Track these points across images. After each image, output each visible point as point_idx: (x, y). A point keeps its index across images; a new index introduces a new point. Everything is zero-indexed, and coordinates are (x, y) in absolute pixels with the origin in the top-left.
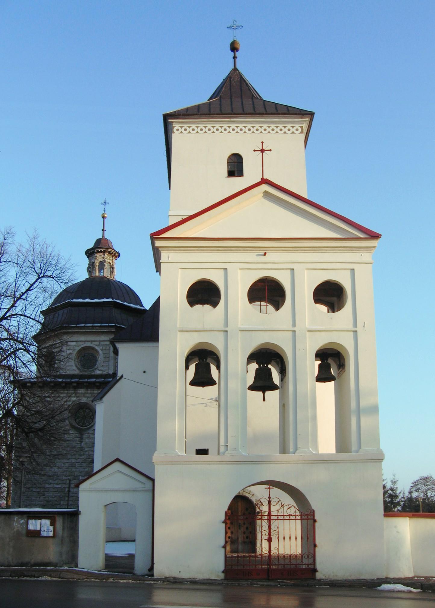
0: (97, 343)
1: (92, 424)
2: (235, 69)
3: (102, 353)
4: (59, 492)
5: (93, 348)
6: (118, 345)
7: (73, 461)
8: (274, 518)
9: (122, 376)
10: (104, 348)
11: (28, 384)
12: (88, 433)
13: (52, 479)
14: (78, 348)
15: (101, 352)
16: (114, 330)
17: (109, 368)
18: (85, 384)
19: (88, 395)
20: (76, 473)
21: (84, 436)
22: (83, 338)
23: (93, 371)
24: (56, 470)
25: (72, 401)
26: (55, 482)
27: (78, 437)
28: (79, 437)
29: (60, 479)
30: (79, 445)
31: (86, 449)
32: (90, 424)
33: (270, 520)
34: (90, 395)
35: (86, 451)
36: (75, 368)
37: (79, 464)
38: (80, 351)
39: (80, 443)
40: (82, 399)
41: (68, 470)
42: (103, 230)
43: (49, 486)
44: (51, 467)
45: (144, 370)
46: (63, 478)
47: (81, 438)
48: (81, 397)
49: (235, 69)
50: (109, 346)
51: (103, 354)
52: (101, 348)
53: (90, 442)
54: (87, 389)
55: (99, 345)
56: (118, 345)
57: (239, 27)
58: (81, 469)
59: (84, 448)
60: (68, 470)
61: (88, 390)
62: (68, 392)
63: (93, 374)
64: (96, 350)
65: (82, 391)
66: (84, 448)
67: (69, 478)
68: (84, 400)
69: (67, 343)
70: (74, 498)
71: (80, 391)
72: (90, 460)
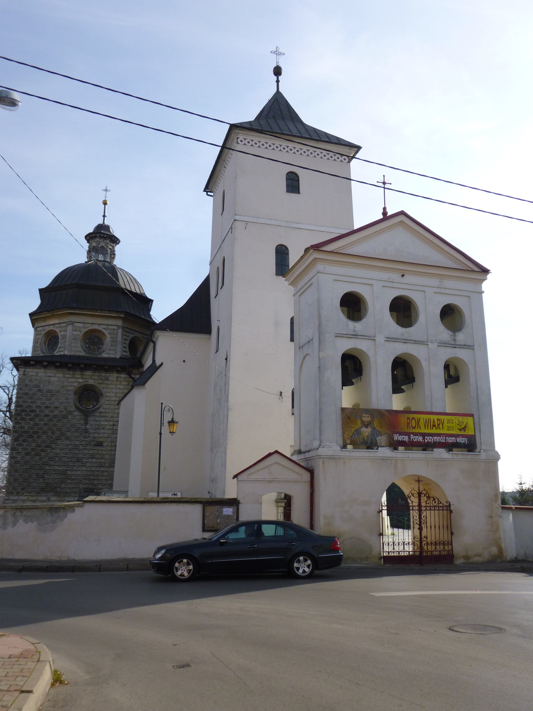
0: (105, 327)
1: (97, 406)
3: (110, 337)
4: (60, 475)
5: (100, 331)
7: (77, 443)
10: (112, 332)
11: (32, 363)
12: (94, 416)
13: (53, 461)
14: (85, 330)
16: (123, 316)
17: (116, 352)
18: (93, 366)
19: (95, 378)
20: (80, 456)
21: (90, 419)
22: (90, 320)
23: (100, 353)
24: (59, 451)
25: (79, 382)
26: (57, 464)
27: (82, 419)
28: (84, 419)
29: (62, 461)
30: (84, 427)
31: (91, 431)
32: (95, 406)
34: (97, 378)
35: (91, 434)
36: (81, 349)
37: (83, 446)
39: (85, 426)
40: (89, 381)
41: (71, 452)
43: (51, 468)
44: (53, 449)
46: (66, 460)
48: (88, 379)
50: (117, 330)
51: (111, 337)
52: (109, 332)
53: (96, 424)
54: (94, 371)
55: (107, 329)
58: (86, 451)
59: (89, 431)
60: (71, 452)
61: (95, 372)
62: (74, 372)
63: (100, 356)
64: (104, 334)
65: (88, 373)
66: (89, 431)
67: (72, 460)
68: (91, 382)
69: (73, 324)
70: (77, 480)
71: (87, 373)
72: (95, 442)
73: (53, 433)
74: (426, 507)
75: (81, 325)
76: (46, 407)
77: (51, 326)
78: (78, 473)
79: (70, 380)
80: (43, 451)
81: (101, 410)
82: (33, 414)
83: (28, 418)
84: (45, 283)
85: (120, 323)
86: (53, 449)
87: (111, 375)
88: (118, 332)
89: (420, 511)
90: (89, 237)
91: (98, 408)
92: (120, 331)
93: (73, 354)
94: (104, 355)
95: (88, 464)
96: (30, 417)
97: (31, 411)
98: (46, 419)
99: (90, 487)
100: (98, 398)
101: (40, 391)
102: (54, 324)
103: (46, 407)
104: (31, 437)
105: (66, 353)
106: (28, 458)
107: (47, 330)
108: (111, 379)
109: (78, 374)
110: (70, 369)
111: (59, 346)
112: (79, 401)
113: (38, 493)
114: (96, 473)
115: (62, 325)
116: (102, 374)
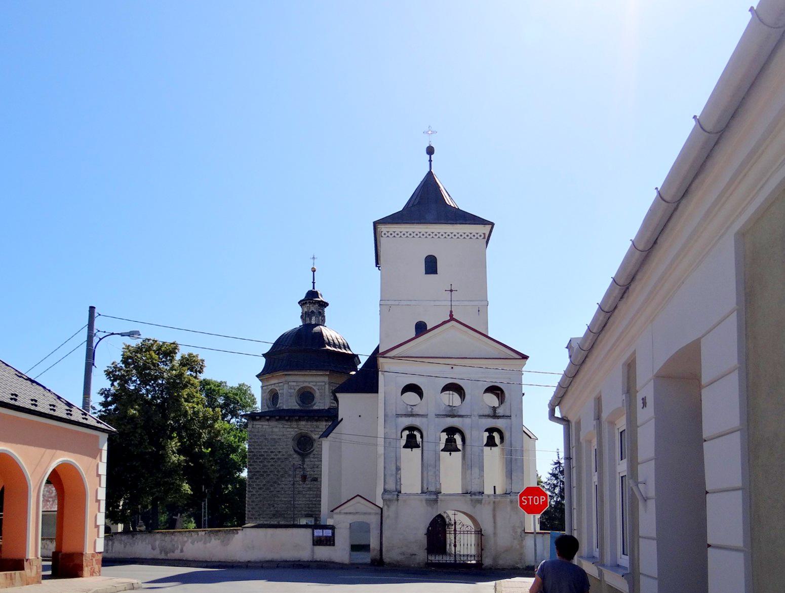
0: (315, 384)
1: (312, 449)
2: (430, 175)
5: (311, 388)
6: (338, 395)
8: (457, 532)
9: (342, 419)
11: (257, 418)
14: (297, 388)
15: (317, 391)
20: (300, 489)
21: (306, 460)
22: (302, 379)
31: (308, 470)
33: (455, 534)
34: (309, 427)
38: (299, 390)
42: (314, 283)
45: (359, 415)
47: (303, 461)
49: (430, 175)
56: (338, 395)
57: (433, 132)
63: (311, 408)
73: (278, 471)
74: (460, 531)
75: (295, 384)
76: (272, 452)
77: (273, 386)
78: (300, 502)
79: (288, 430)
80: (271, 486)
81: (315, 452)
82: (262, 458)
83: (258, 461)
84: (267, 348)
85: (326, 379)
86: (279, 484)
87: (321, 423)
88: (325, 387)
89: (455, 534)
90: (302, 303)
91: (313, 451)
92: (327, 386)
93: (290, 408)
94: (315, 408)
95: (307, 496)
96: (260, 460)
97: (260, 455)
98: (272, 461)
99: (310, 513)
100: (312, 443)
101: (266, 439)
102: (275, 384)
103: (272, 452)
104: (262, 475)
105: (285, 408)
106: (261, 492)
107: (270, 389)
108: (320, 427)
109: (294, 424)
110: (287, 421)
111: (279, 401)
112: (298, 446)
113: (271, 518)
114: (314, 502)
115: (280, 384)
116: (313, 424)
